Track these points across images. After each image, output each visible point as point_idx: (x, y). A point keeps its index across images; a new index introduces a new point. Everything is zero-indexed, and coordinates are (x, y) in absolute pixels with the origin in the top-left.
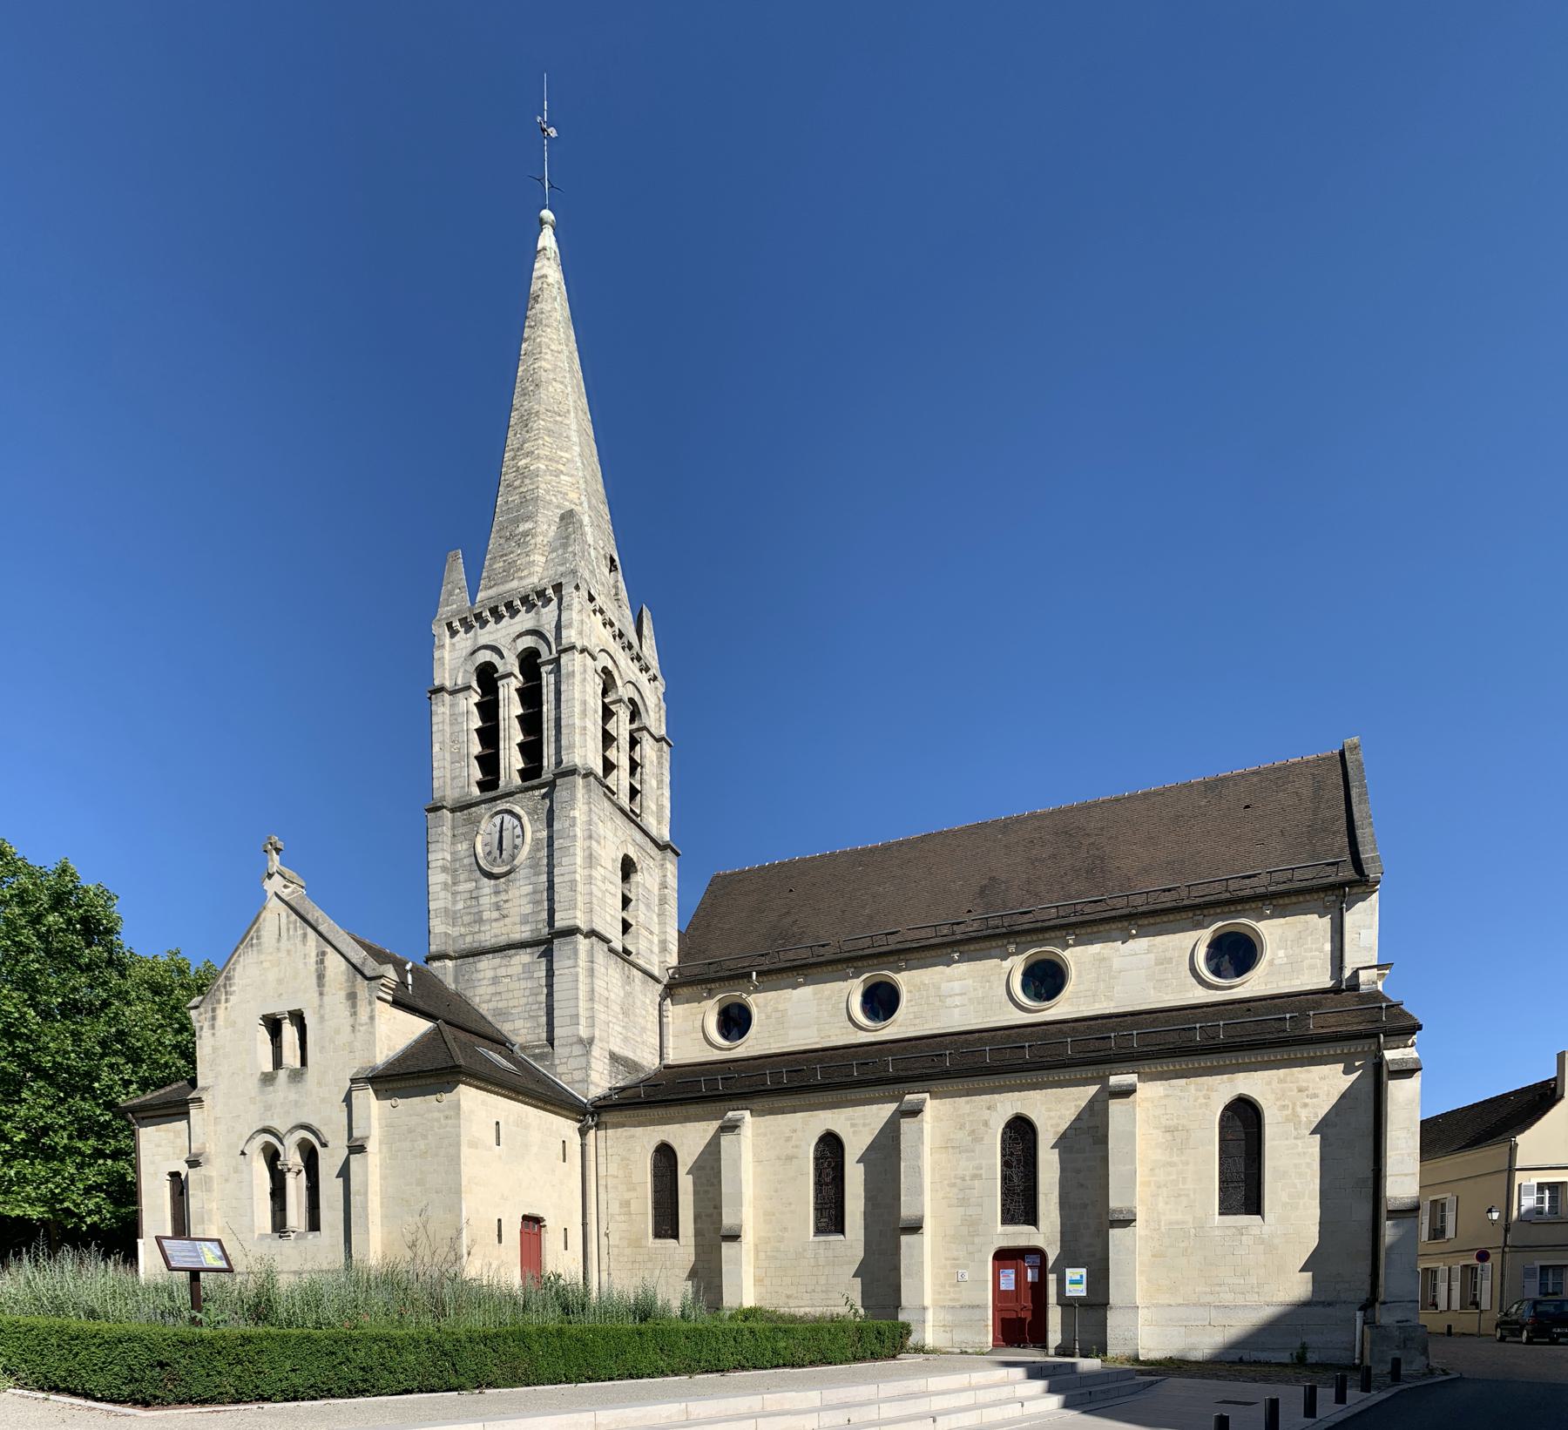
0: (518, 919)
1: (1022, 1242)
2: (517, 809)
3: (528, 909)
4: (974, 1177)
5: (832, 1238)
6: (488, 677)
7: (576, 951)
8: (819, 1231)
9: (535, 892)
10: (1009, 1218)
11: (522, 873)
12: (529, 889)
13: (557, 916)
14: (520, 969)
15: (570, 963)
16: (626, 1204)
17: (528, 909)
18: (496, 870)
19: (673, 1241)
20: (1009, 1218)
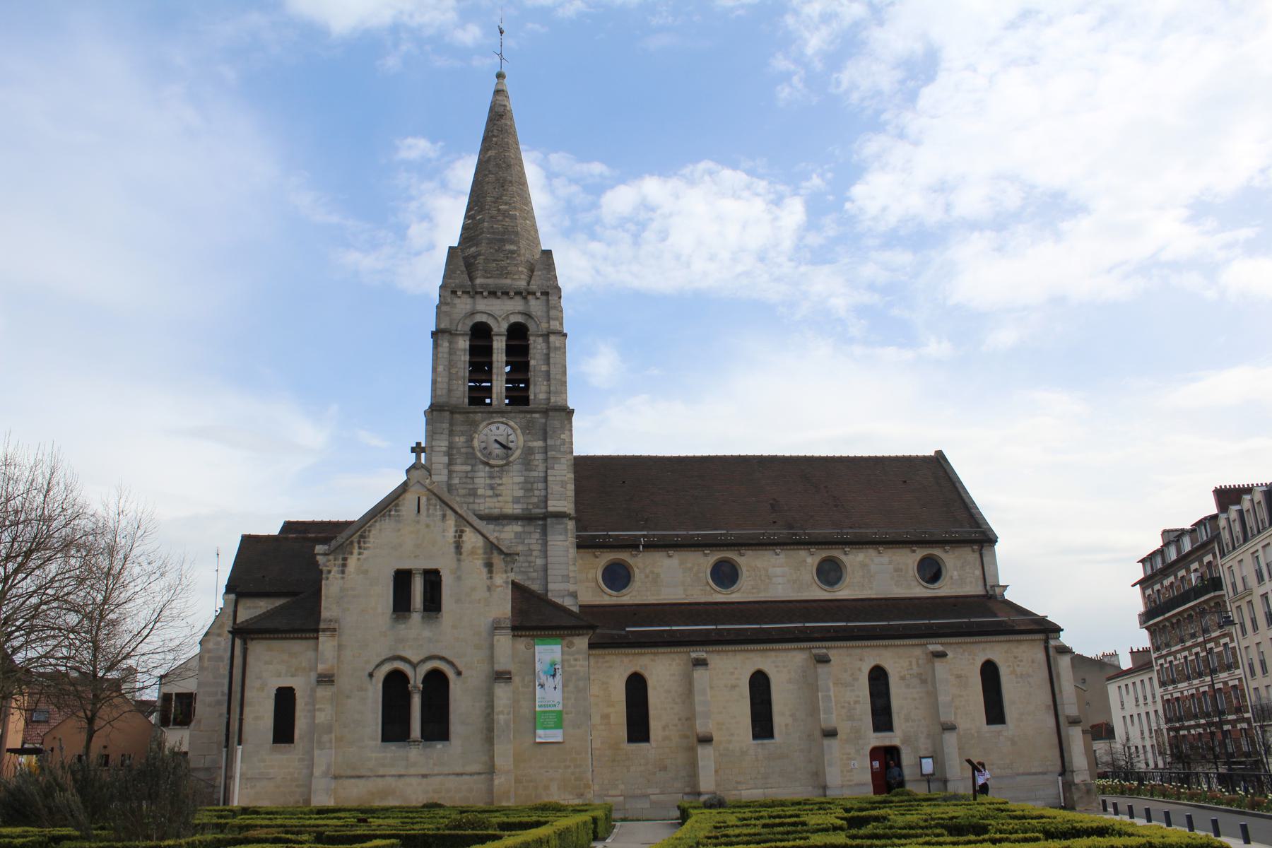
0: (510, 499)
1: (887, 743)
2: (512, 423)
3: (520, 493)
4: (856, 702)
5: (765, 741)
6: (481, 334)
7: (566, 530)
8: (755, 737)
9: (526, 482)
10: (877, 728)
11: (516, 467)
12: (522, 479)
13: (550, 503)
14: (512, 536)
15: (562, 537)
16: (606, 717)
17: (520, 493)
18: (492, 462)
19: (643, 745)
20: (877, 728)
